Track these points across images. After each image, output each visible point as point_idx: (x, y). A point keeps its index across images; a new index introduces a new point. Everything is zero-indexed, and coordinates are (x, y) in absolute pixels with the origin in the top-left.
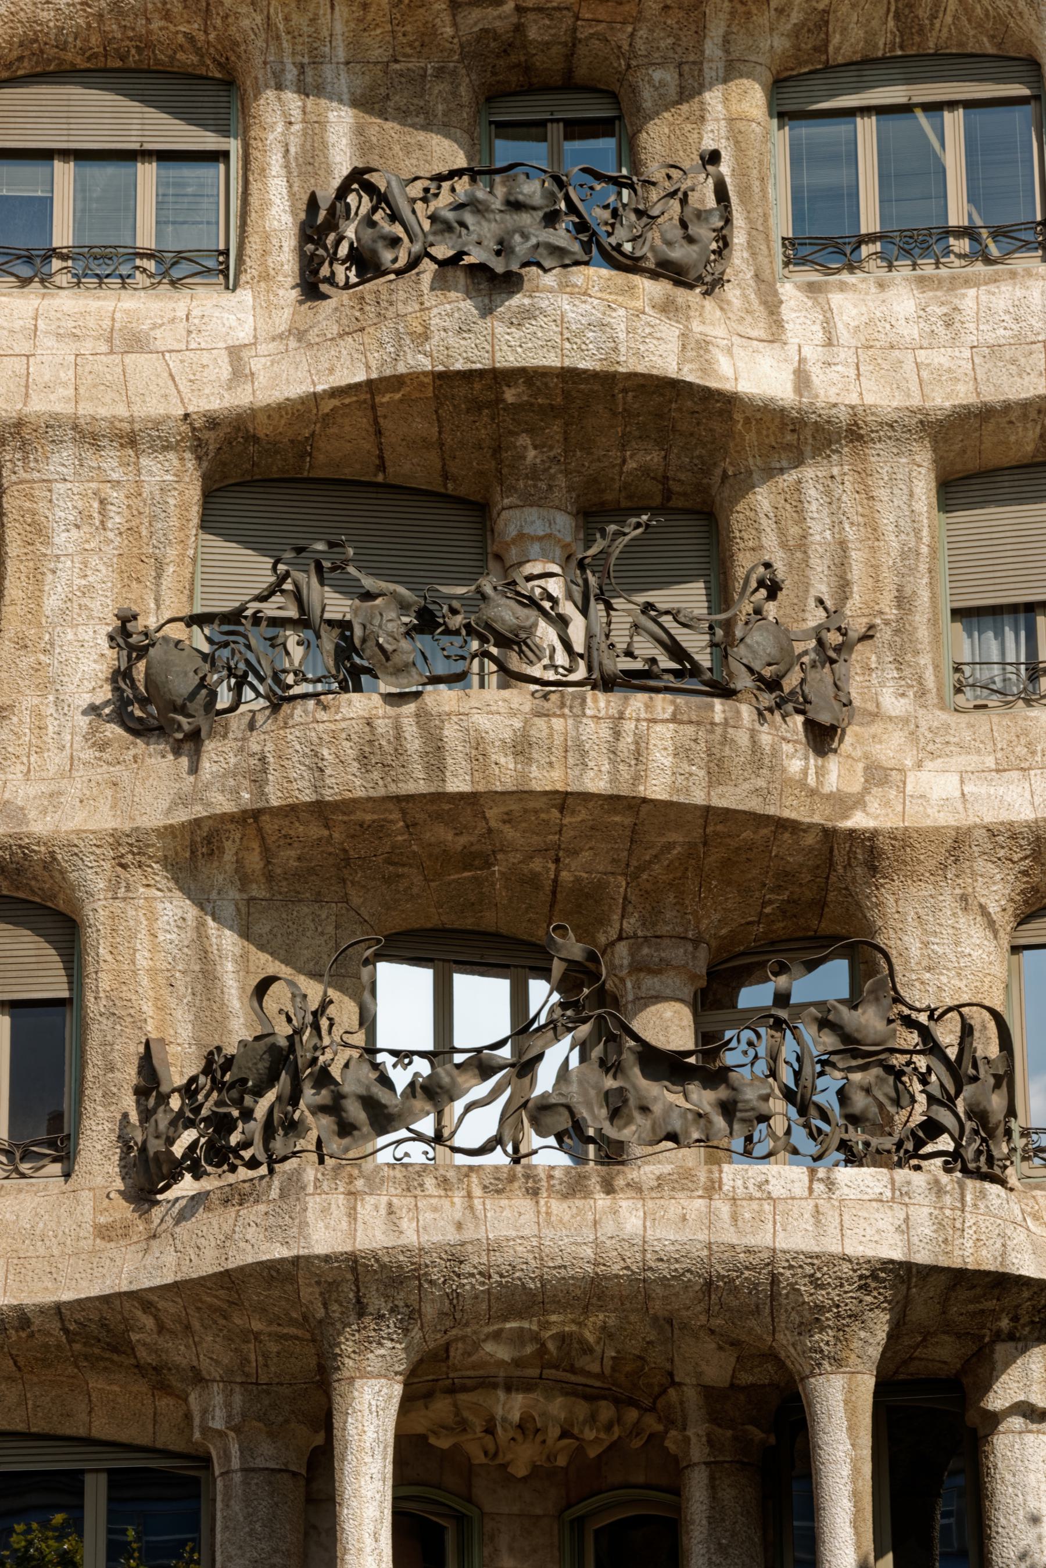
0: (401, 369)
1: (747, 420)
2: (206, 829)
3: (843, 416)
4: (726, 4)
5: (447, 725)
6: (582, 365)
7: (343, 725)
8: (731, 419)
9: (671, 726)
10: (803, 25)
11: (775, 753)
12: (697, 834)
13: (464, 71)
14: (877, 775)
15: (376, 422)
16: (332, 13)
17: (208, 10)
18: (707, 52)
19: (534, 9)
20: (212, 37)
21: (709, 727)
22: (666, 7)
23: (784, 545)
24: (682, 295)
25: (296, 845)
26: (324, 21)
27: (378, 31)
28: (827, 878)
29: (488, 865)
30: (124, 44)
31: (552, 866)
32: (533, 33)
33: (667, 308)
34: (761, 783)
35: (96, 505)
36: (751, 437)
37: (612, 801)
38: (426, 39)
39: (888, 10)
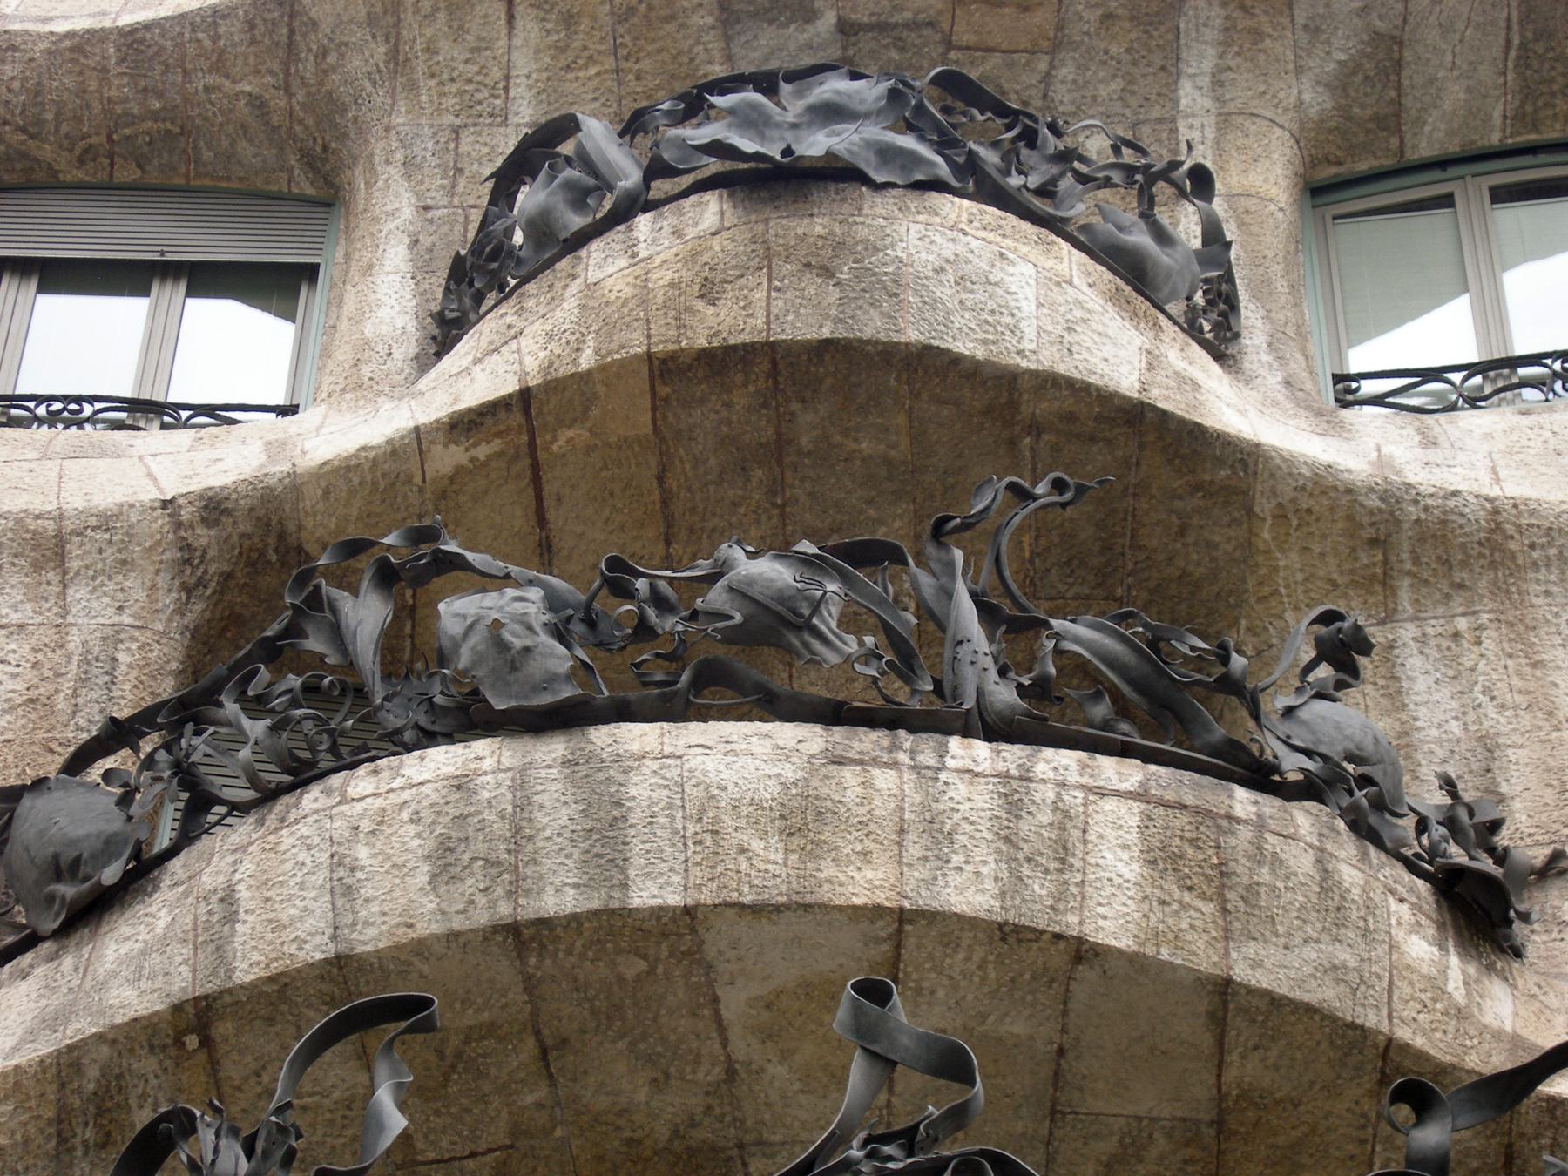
1: (1281, 516)
2: (93, 1072)
3: (1477, 513)
4: (1217, 11)
5: (634, 778)
7: (406, 795)
8: (1250, 511)
9: (1136, 806)
10: (1358, 67)
12: (1201, 1090)
15: (542, 521)
16: (510, 35)
17: (291, 44)
18: (1184, 102)
19: (870, 27)
20: (300, 96)
22: (1108, 17)
27: (593, 71)
34: (1345, 956)
37: (1007, 935)
39: (1508, 42)
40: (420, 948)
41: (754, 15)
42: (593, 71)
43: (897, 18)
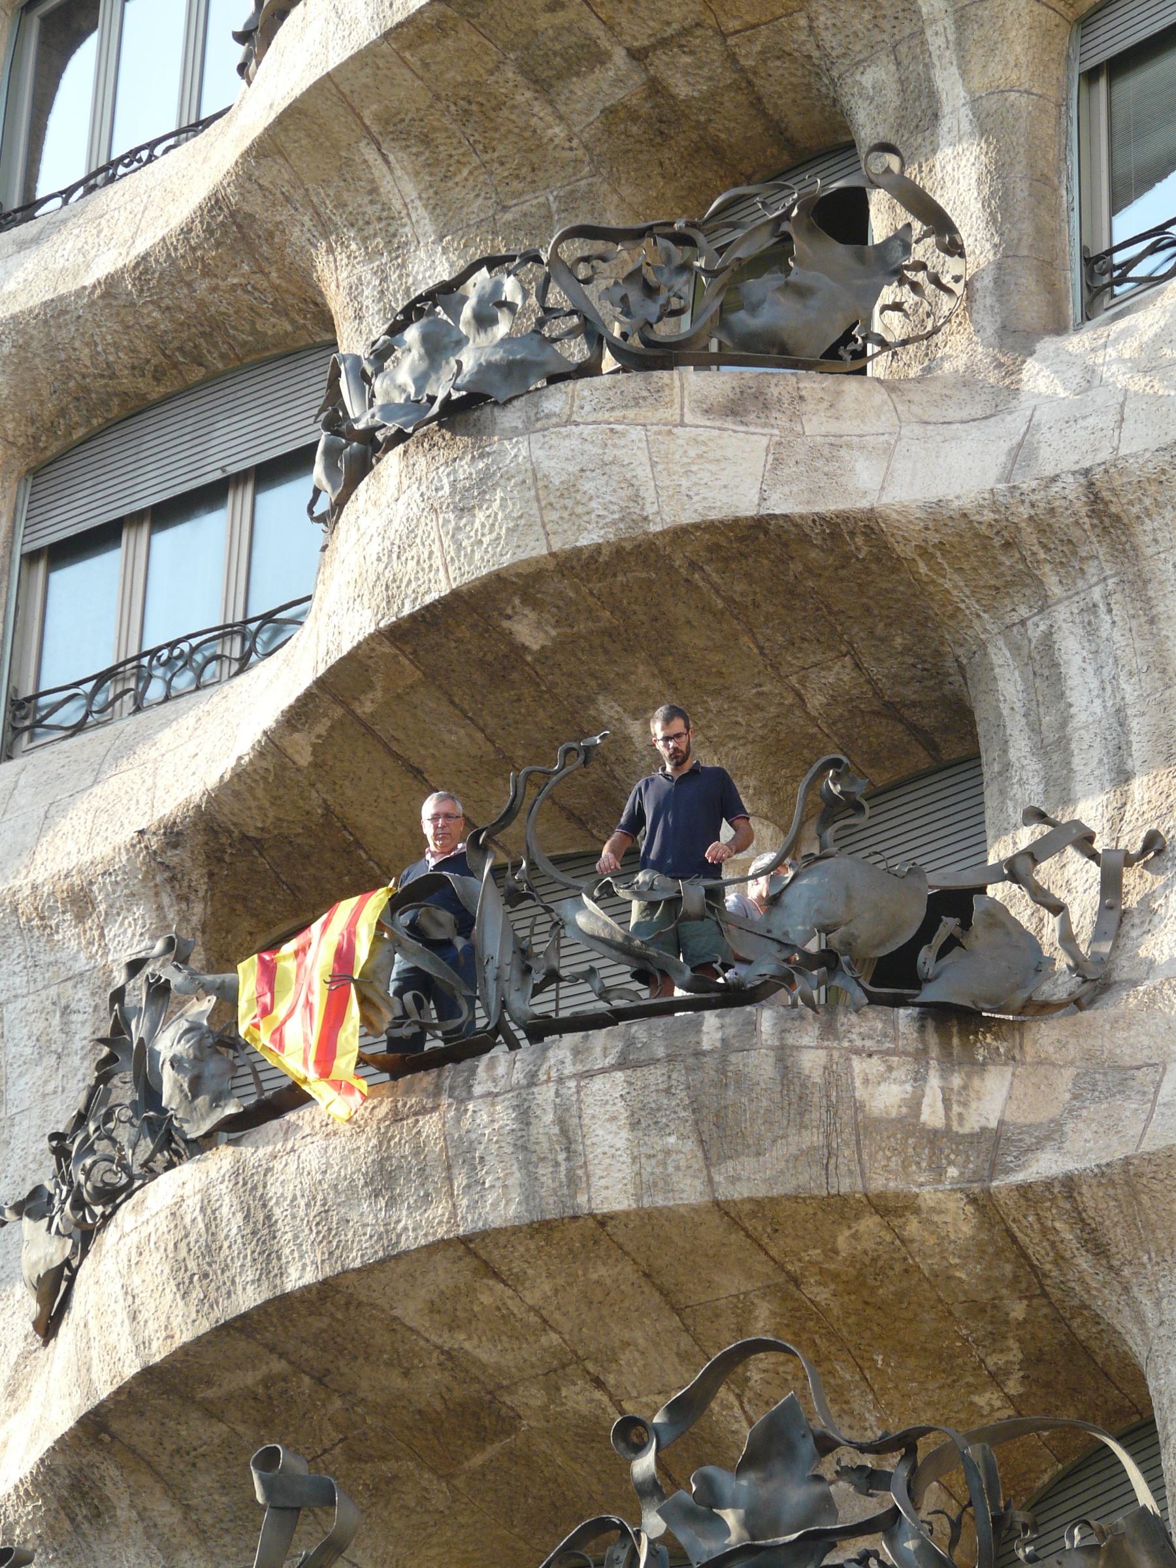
0: (346, 648)
6: (584, 541)
9: (619, 1076)
11: (836, 1078)
13: (605, 186)
14: (1110, 1078)
19: (654, 47)
21: (691, 1061)
23: (1042, 750)
24: (782, 382)
25: (201, 1464)
26: (386, 185)
27: (465, 172)
28: (1045, 1295)
29: (508, 1423)
30: (184, 335)
31: (598, 1395)
32: (682, 89)
33: (733, 409)
34: (813, 1138)
35: (56, 1020)
36: (952, 583)
38: (534, 157)
40: (186, 1351)
41: (559, 77)
42: (465, 172)
43: (669, 31)
